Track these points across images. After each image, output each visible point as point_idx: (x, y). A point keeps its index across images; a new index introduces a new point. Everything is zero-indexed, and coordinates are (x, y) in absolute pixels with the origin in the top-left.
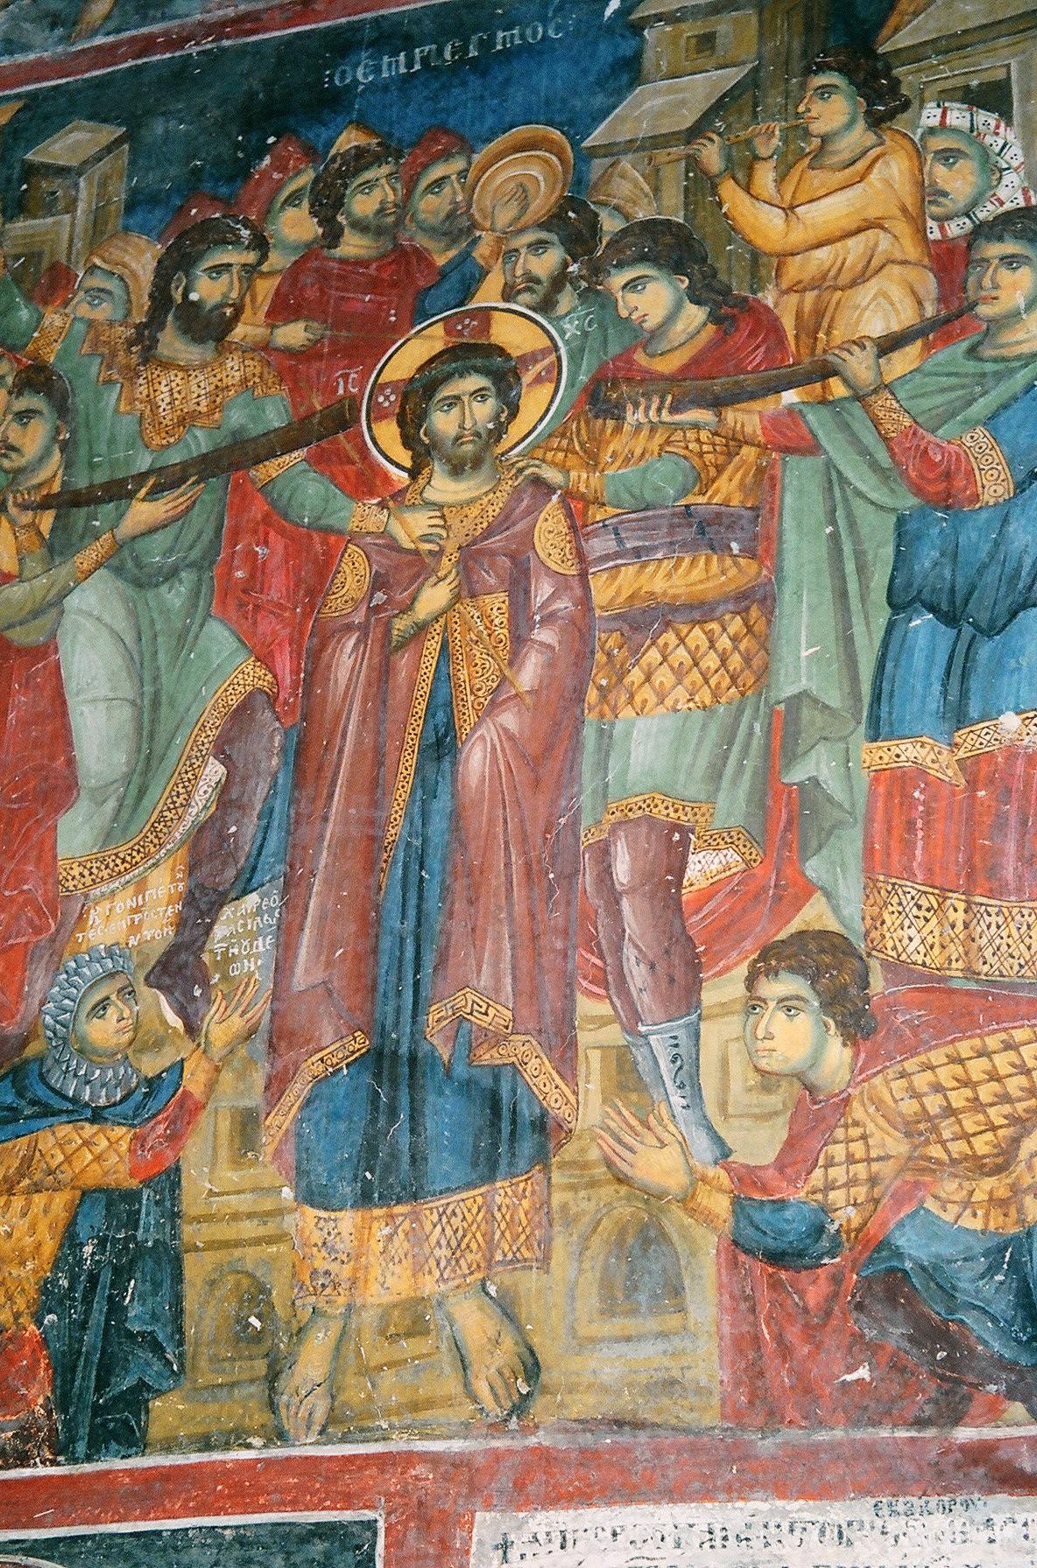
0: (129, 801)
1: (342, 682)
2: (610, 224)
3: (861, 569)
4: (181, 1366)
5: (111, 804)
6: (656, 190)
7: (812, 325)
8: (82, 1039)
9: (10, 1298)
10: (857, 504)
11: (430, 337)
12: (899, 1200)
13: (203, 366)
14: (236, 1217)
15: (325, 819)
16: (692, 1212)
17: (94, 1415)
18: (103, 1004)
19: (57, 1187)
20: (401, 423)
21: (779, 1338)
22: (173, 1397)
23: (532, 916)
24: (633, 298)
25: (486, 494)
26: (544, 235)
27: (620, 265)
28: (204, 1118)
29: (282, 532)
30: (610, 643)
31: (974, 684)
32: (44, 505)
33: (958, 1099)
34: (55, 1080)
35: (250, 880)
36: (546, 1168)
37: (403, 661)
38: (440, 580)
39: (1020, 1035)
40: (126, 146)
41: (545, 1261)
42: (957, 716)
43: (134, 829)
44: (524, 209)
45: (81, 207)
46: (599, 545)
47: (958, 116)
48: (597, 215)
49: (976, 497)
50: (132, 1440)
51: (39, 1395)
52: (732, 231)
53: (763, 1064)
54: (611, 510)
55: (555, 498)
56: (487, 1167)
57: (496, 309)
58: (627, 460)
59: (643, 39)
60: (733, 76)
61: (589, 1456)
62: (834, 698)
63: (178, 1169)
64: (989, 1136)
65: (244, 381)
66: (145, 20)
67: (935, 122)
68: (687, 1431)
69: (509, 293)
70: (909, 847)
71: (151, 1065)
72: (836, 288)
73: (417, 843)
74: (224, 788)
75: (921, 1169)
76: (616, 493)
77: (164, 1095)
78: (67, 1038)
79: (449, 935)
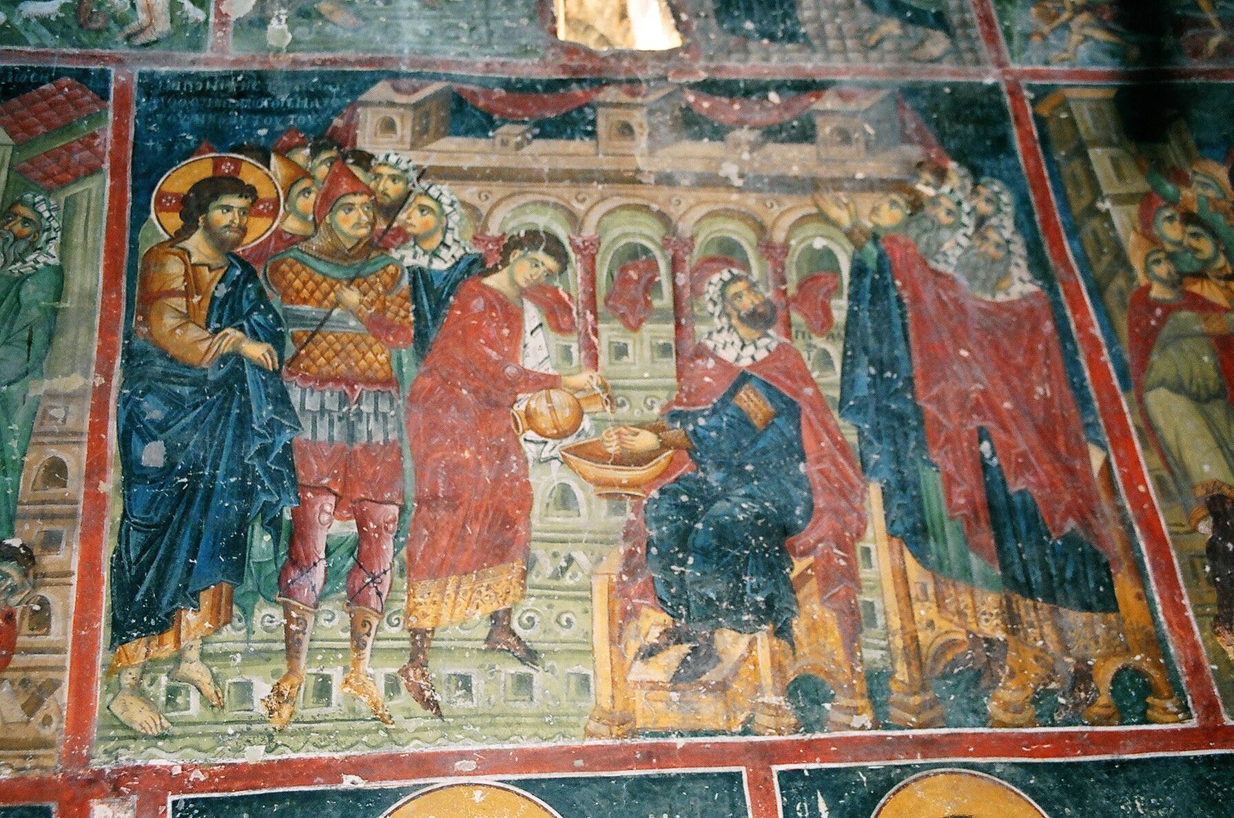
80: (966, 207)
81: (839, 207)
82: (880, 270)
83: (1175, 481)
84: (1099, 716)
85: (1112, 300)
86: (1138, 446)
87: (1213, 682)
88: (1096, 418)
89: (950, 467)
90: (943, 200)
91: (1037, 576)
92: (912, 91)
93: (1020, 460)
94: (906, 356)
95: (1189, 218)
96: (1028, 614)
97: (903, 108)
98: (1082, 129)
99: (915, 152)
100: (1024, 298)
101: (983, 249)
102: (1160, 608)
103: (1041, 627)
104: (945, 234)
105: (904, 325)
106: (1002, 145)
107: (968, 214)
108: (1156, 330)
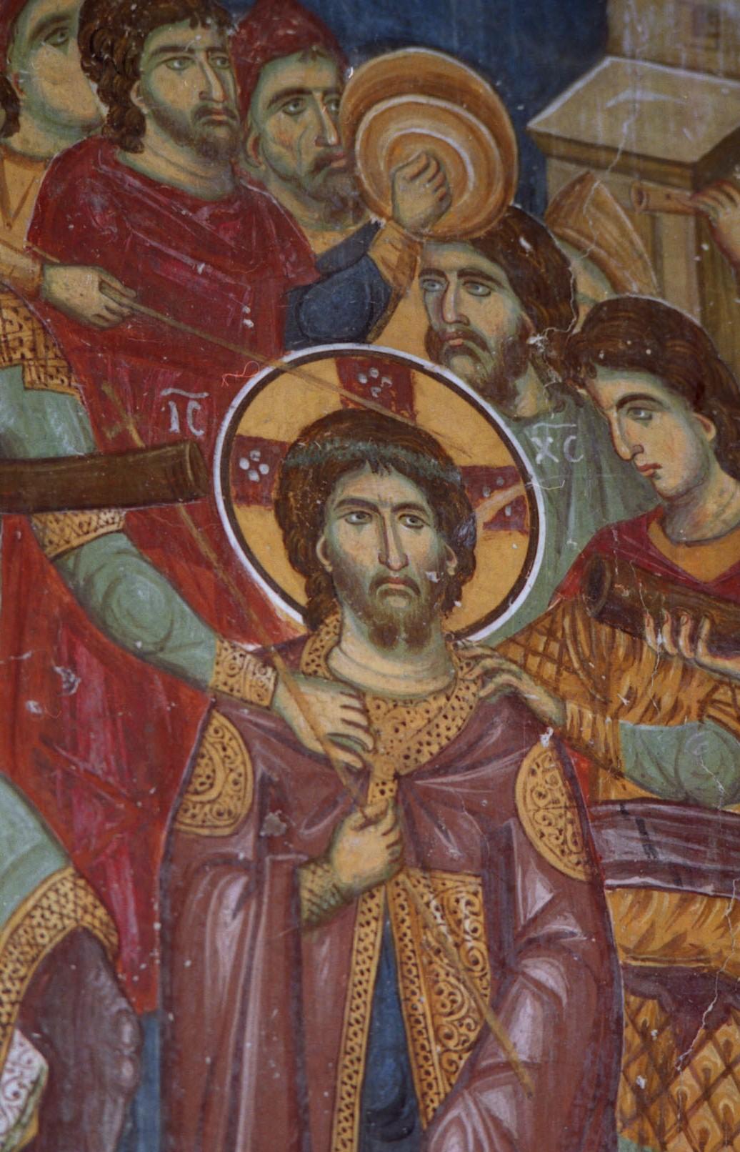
1: (226, 959)
2: (590, 289)
6: (656, 254)
11: (312, 378)
24: (633, 427)
25: (436, 694)
26: (485, 265)
29: (101, 653)
37: (323, 951)
38: (369, 822)
48: (566, 262)
55: (545, 739)
57: (420, 368)
58: (652, 711)
69: (435, 344)
76: (638, 764)
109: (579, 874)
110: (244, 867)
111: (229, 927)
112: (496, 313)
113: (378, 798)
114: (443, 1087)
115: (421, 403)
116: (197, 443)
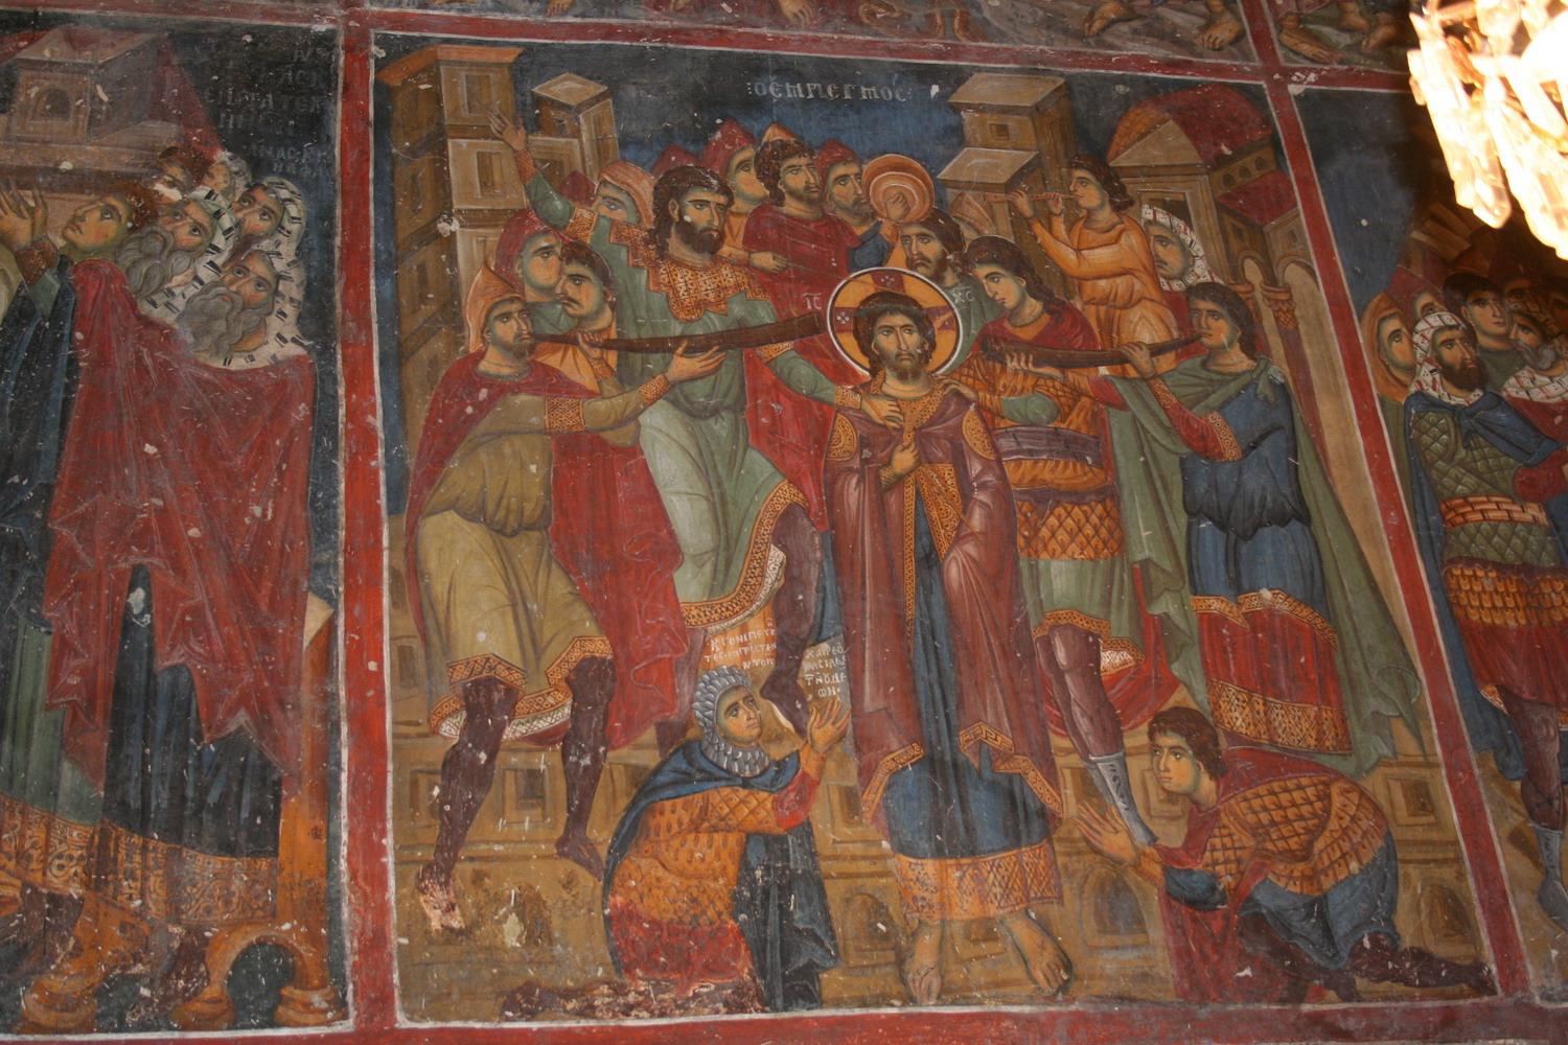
0: (721, 567)
1: (854, 507)
2: (969, 235)
3: (1165, 488)
4: (836, 952)
5: (708, 568)
6: (993, 218)
7: (1109, 326)
8: (724, 730)
9: (712, 902)
10: (1155, 445)
12: (1256, 872)
13: (706, 269)
14: (854, 858)
15: (864, 599)
16: (1141, 873)
17: (784, 982)
18: (734, 708)
19: (729, 830)
20: (857, 337)
21: (1201, 950)
22: (834, 972)
23: (1012, 679)
24: (992, 284)
27: (981, 262)
28: (820, 791)
29: (790, 398)
30: (1024, 509)
31: (1243, 569)
32: (607, 345)
33: (1277, 815)
34: (711, 755)
35: (820, 633)
36: (1050, 841)
37: (892, 499)
39: (1304, 781)
40: (610, 100)
41: (1060, 898)
42: (1238, 587)
43: (729, 588)
44: (908, 209)
45: (585, 137)
46: (1005, 444)
47: (1162, 218)
49: (1221, 455)
50: (812, 998)
51: (745, 969)
52: (1046, 257)
53: (1166, 785)
54: (1010, 423)
55: (972, 407)
56: (1015, 839)
58: (1013, 392)
59: (961, 118)
60: (1026, 157)
61: (1108, 1018)
62: (1167, 565)
63: (809, 824)
64: (1296, 839)
65: (737, 286)
66: (602, 14)
67: (1151, 217)
68: (1159, 1003)
69: (911, 264)
70: (1226, 664)
71: (777, 752)
72: (1116, 308)
73: (927, 622)
74: (787, 568)
75: (1264, 858)
77: (790, 773)
78: (714, 728)
79: (961, 686)
80: (227, 221)
81: (20, 214)
82: (56, 316)
83: (428, 657)
84: (198, 1015)
85: (415, 372)
86: (386, 601)
87: (395, 964)
88: (336, 557)
89: (71, 627)
90: (192, 209)
91: (161, 798)
92: (189, 38)
93: (188, 619)
94: (55, 451)
95: (576, 251)
96: (129, 857)
97: (168, 63)
98: (446, 105)
99: (165, 133)
100: (276, 365)
101: (233, 288)
102: (344, 851)
103: (145, 878)
104: (181, 261)
105: (66, 402)
106: (314, 126)
107: (226, 232)
108: (472, 420)
109: (992, 458)
110: (857, 471)
111: (853, 494)
112: (933, 248)
113: (908, 438)
114: (947, 545)
115: (907, 286)
116: (818, 313)
